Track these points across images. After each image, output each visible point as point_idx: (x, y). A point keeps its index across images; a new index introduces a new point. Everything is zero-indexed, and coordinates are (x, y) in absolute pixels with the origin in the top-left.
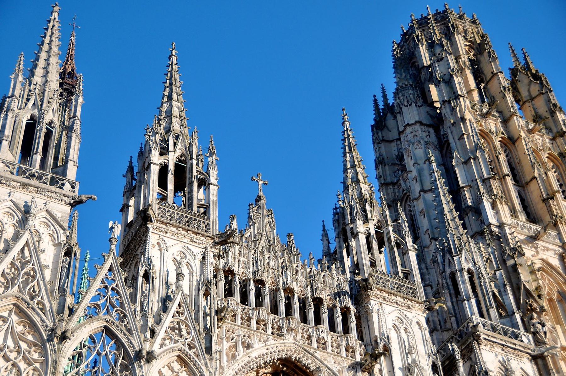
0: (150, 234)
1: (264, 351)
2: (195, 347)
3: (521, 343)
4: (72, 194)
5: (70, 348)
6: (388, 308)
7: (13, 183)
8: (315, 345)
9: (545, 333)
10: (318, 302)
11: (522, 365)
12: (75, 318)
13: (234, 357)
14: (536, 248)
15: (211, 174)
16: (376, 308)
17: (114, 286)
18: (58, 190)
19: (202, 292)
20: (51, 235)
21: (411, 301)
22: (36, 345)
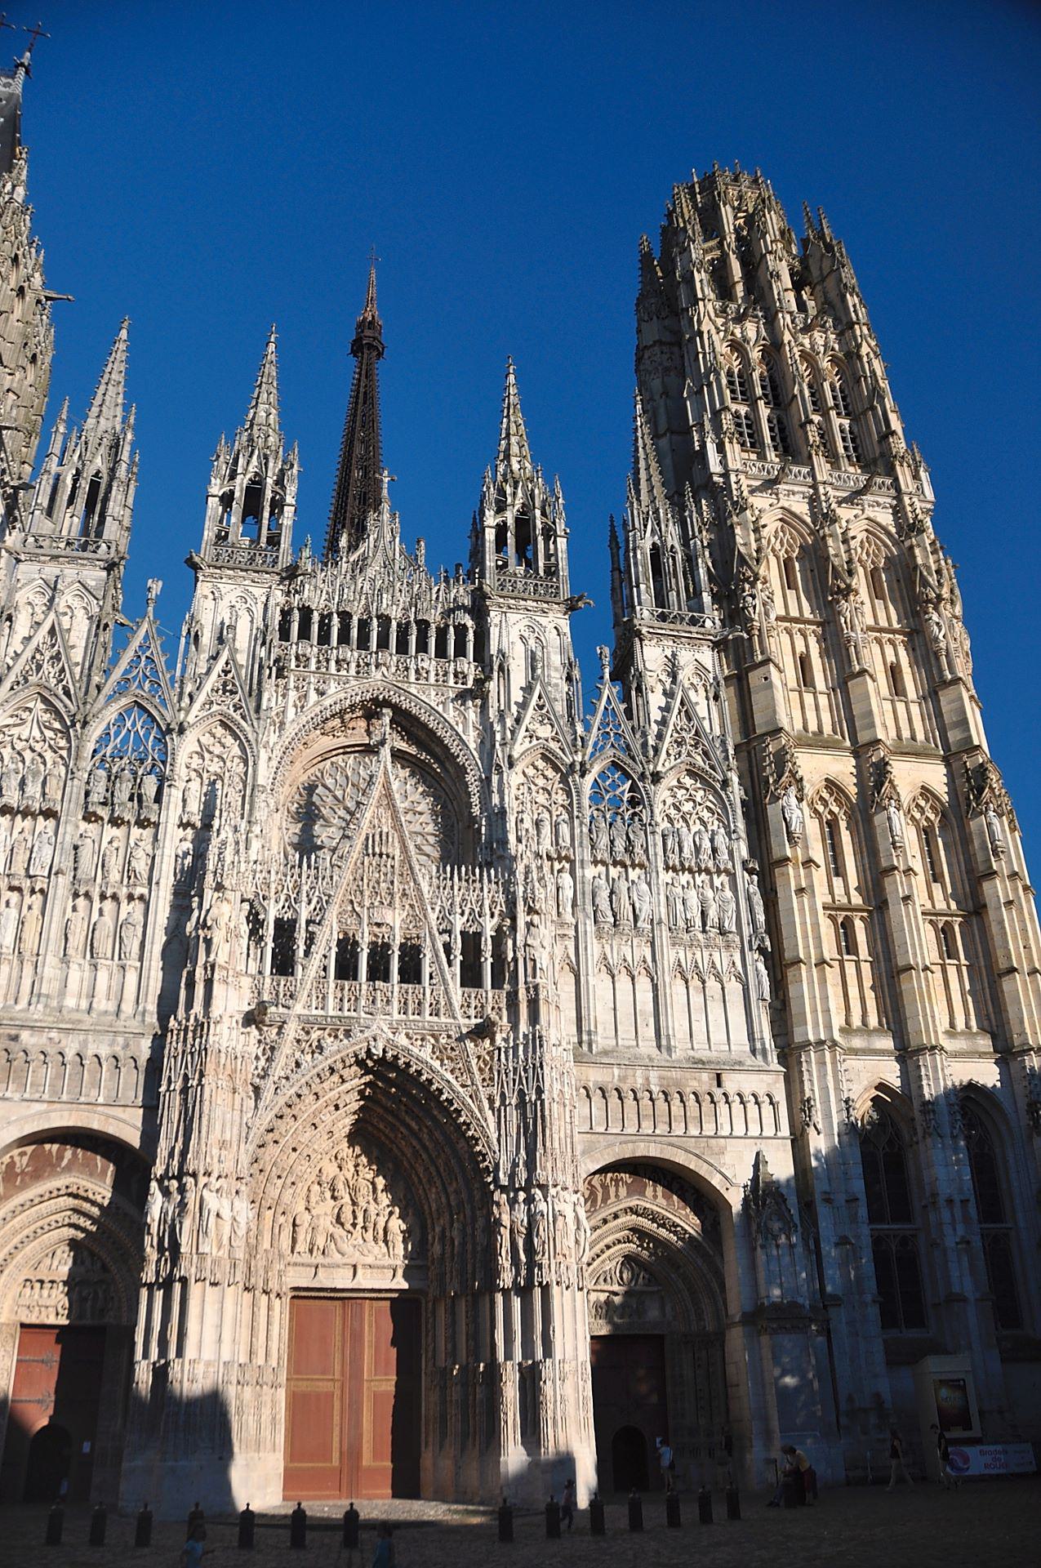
0: (199, 584)
1: (342, 695)
2: (241, 707)
3: (702, 630)
4: (104, 557)
5: (96, 730)
6: (513, 617)
7: (42, 558)
8: (412, 678)
9: (755, 607)
10: (423, 625)
11: (698, 656)
12: (102, 698)
13: (303, 707)
14: (777, 494)
15: (288, 492)
16: (496, 620)
17: (148, 654)
18: (91, 555)
19: (259, 642)
20: (85, 608)
21: (547, 602)
22: (61, 732)
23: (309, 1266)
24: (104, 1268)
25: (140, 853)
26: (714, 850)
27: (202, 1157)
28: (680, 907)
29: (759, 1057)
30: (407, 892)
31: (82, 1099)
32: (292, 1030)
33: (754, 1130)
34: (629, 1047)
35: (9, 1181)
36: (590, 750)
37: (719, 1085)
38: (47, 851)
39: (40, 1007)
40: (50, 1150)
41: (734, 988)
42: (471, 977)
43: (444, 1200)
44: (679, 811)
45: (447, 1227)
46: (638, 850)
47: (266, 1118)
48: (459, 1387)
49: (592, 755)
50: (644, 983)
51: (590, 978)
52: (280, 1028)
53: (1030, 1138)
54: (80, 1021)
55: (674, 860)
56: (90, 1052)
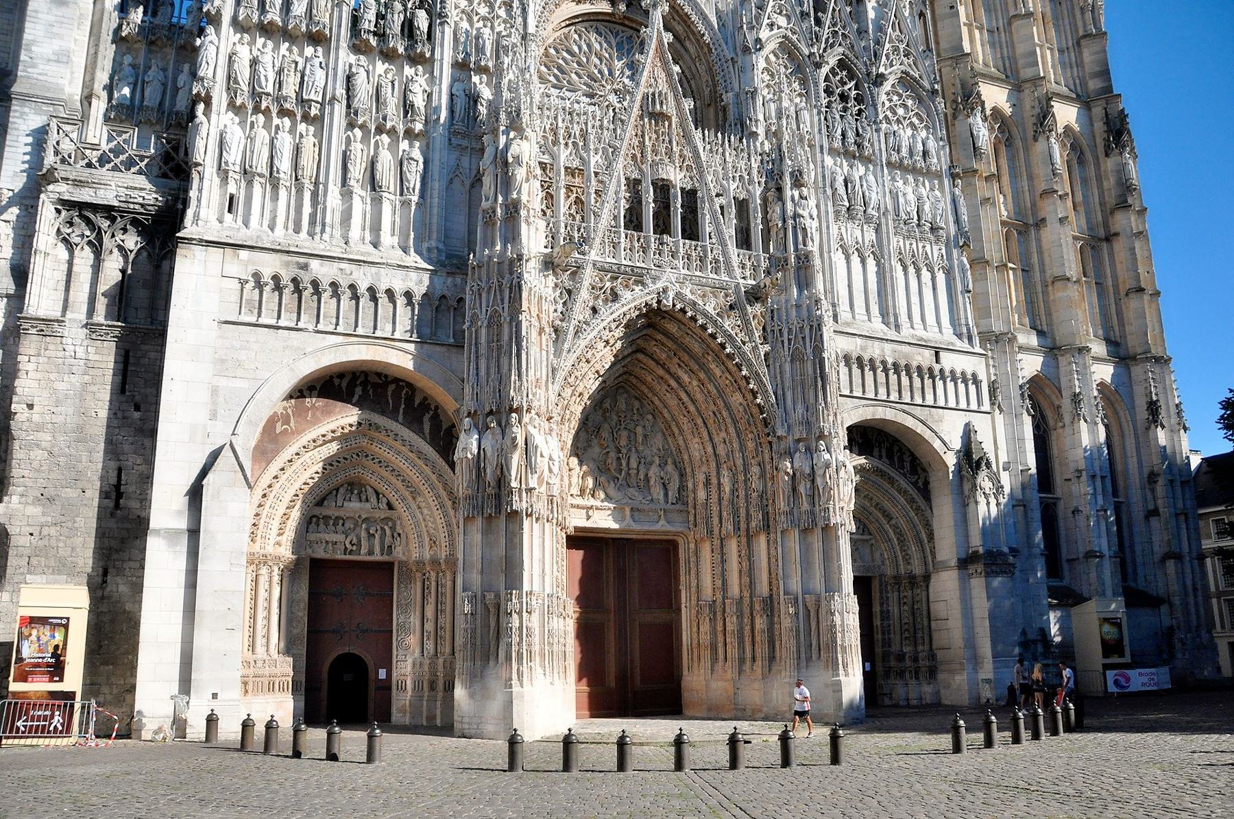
23: (583, 508)
24: (390, 506)
25: (416, 88)
26: (925, 154)
27: (525, 395)
28: (901, 200)
29: (966, 341)
30: (685, 152)
31: (378, 334)
32: (589, 276)
33: (963, 405)
34: (863, 321)
35: (300, 415)
36: (823, 46)
37: (937, 361)
38: (320, 75)
39: (326, 236)
40: (340, 385)
41: (941, 277)
42: (744, 241)
43: (710, 449)
44: (895, 113)
45: (714, 473)
46: (866, 144)
47: (567, 361)
48: (735, 618)
49: (825, 50)
50: (871, 263)
51: (832, 254)
52: (574, 274)
53: (1148, 429)
54: (369, 254)
55: (895, 157)
56: (382, 287)
